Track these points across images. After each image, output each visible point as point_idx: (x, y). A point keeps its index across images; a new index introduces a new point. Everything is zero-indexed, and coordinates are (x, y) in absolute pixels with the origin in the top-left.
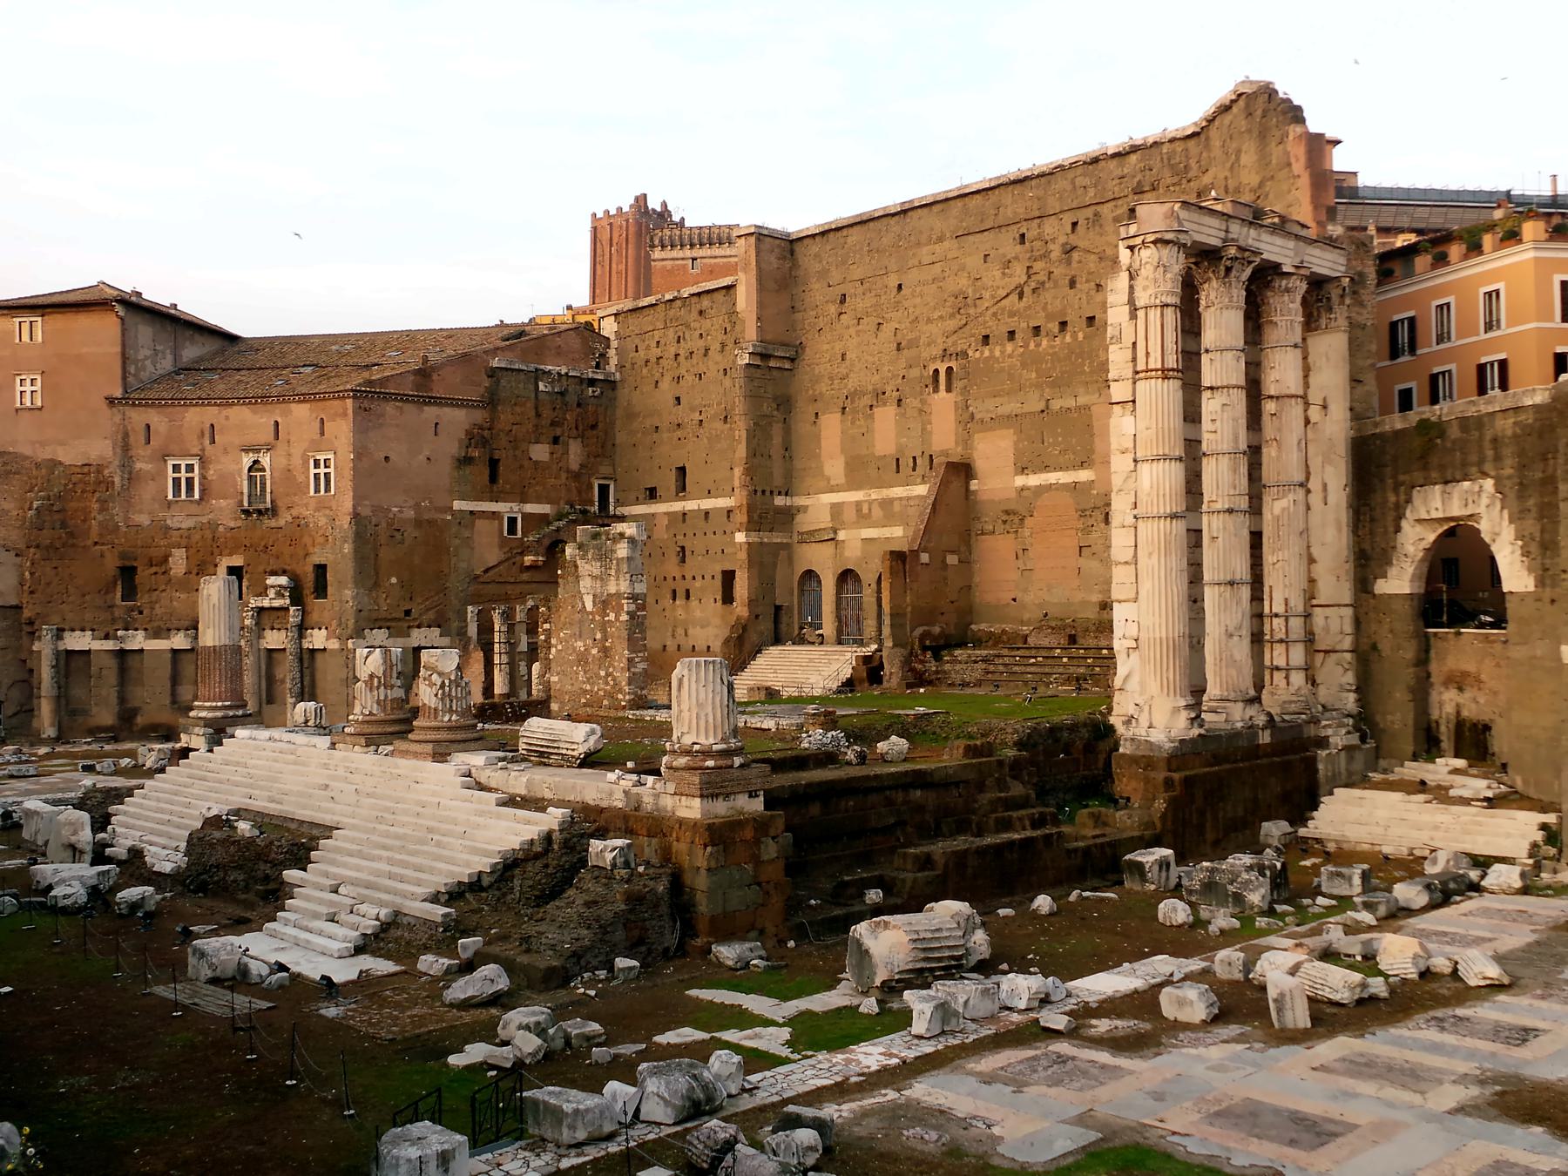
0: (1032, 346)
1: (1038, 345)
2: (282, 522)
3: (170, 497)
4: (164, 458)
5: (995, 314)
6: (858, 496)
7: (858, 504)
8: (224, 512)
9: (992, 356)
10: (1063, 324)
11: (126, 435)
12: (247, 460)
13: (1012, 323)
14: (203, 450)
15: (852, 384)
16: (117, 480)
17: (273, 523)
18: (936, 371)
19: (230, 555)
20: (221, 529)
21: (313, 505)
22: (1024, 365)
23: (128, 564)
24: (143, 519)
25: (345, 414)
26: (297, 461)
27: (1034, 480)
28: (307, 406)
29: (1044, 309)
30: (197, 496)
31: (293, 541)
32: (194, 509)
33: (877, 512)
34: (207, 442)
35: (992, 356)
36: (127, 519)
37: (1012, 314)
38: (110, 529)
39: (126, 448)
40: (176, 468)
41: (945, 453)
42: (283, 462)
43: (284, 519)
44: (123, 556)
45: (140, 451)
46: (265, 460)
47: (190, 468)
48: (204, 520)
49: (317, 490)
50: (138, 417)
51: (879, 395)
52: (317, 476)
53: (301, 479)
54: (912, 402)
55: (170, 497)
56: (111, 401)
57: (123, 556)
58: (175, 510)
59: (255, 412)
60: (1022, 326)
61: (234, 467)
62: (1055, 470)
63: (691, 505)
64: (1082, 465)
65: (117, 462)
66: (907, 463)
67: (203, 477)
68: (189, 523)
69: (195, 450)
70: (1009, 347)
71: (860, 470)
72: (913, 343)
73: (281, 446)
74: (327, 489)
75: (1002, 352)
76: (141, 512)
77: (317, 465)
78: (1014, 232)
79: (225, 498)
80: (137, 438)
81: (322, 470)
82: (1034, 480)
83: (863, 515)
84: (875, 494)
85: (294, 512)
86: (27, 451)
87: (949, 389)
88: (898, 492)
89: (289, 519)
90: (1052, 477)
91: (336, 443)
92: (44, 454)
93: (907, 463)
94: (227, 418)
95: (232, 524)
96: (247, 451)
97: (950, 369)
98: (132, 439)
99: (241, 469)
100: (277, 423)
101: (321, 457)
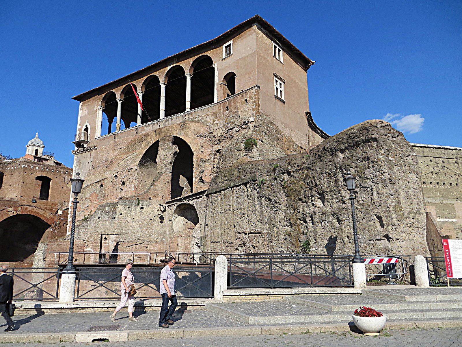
0: (437, 187)
1: (439, 187)
5: (426, 177)
9: (426, 187)
10: (444, 184)
13: (431, 180)
22: (436, 191)
27: (442, 220)
29: (439, 179)
35: (426, 187)
37: (432, 178)
60: (434, 182)
62: (447, 218)
64: (454, 217)
70: (431, 186)
75: (430, 187)
78: (429, 159)
82: (442, 220)
90: (447, 220)
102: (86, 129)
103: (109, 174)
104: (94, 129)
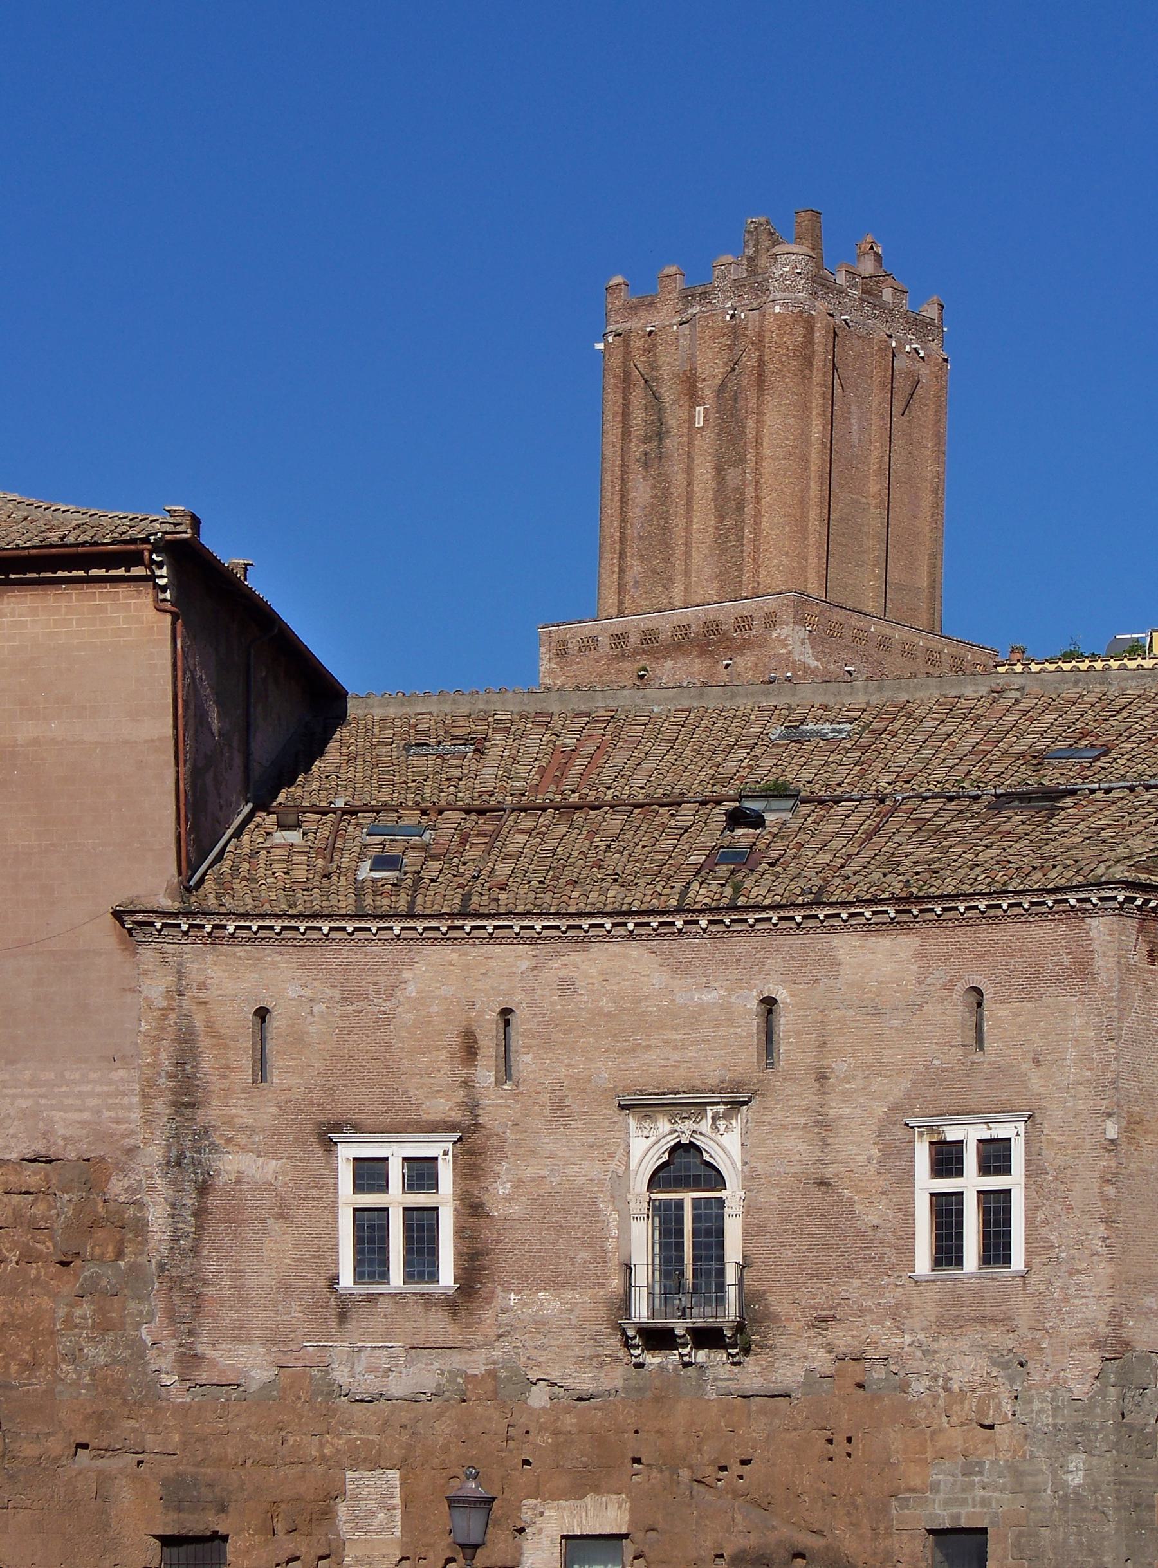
2: (789, 1375)
3: (347, 1279)
4: (327, 1136)
8: (552, 1339)
11: (186, 1047)
12: (647, 1145)
14: (472, 1107)
16: (157, 1215)
17: (752, 1374)
19: (576, 1492)
20: (538, 1397)
21: (926, 1305)
23: (196, 1524)
24: (253, 1364)
25: (1082, 971)
26: (857, 1149)
28: (906, 944)
30: (447, 1275)
31: (838, 1442)
32: (438, 1325)
34: (485, 1074)
36: (189, 1361)
38: (124, 1393)
39: (187, 1098)
40: (370, 1174)
42: (797, 1149)
43: (793, 1360)
44: (177, 1493)
45: (233, 1107)
46: (725, 1145)
47: (421, 1174)
48: (477, 1364)
49: (947, 1251)
50: (230, 979)
52: (947, 1211)
53: (874, 1213)
55: (347, 1279)
56: (132, 922)
57: (177, 1493)
58: (365, 1326)
59: (680, 968)
61: (592, 1169)
65: (155, 1153)
67: (472, 1209)
68: (410, 1378)
69: (443, 1107)
73: (790, 1099)
74: (996, 1248)
76: (239, 1334)
77: (947, 1160)
79: (558, 1282)
80: (224, 1066)
81: (971, 1183)
85: (844, 1338)
89: (822, 1361)
91: (1036, 1082)
94: (567, 987)
95: (585, 1380)
96: (644, 1107)
98: (207, 1062)
99: (621, 1179)
100: (769, 1003)
101: (969, 1135)
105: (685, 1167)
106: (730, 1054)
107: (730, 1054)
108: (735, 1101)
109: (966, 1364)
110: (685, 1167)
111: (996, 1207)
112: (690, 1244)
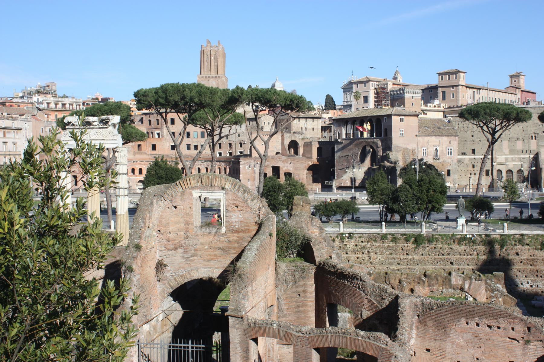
6: (513, 156)
7: (512, 158)
15: (511, 136)
17: (439, 161)
18: (532, 136)
26: (444, 149)
33: (517, 160)
41: (534, 150)
43: (441, 160)
51: (518, 139)
52: (448, 152)
53: (445, 152)
54: (526, 141)
63: (476, 157)
66: (524, 151)
71: (512, 152)
72: (527, 130)
74: (451, 154)
77: (448, 150)
81: (450, 151)
83: (513, 160)
84: (516, 156)
86: (401, 145)
87: (535, 139)
88: (522, 156)
92: (405, 146)
93: (524, 151)
97: (535, 136)
101: (450, 148)
102: (339, 133)
103: (350, 154)
104: (342, 134)
105: (436, 149)
106: (438, 143)
107: (438, 143)
108: (438, 146)
109: (449, 161)
110: (436, 149)
111: (451, 152)
112: (436, 154)
